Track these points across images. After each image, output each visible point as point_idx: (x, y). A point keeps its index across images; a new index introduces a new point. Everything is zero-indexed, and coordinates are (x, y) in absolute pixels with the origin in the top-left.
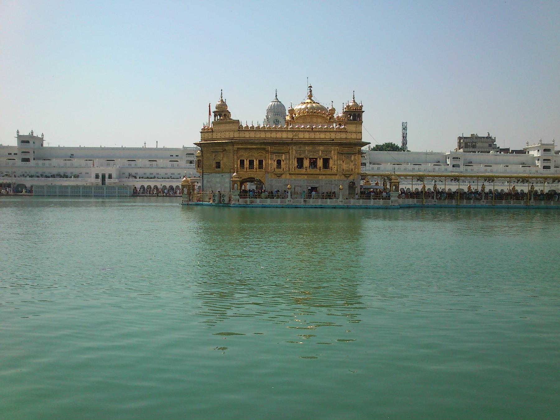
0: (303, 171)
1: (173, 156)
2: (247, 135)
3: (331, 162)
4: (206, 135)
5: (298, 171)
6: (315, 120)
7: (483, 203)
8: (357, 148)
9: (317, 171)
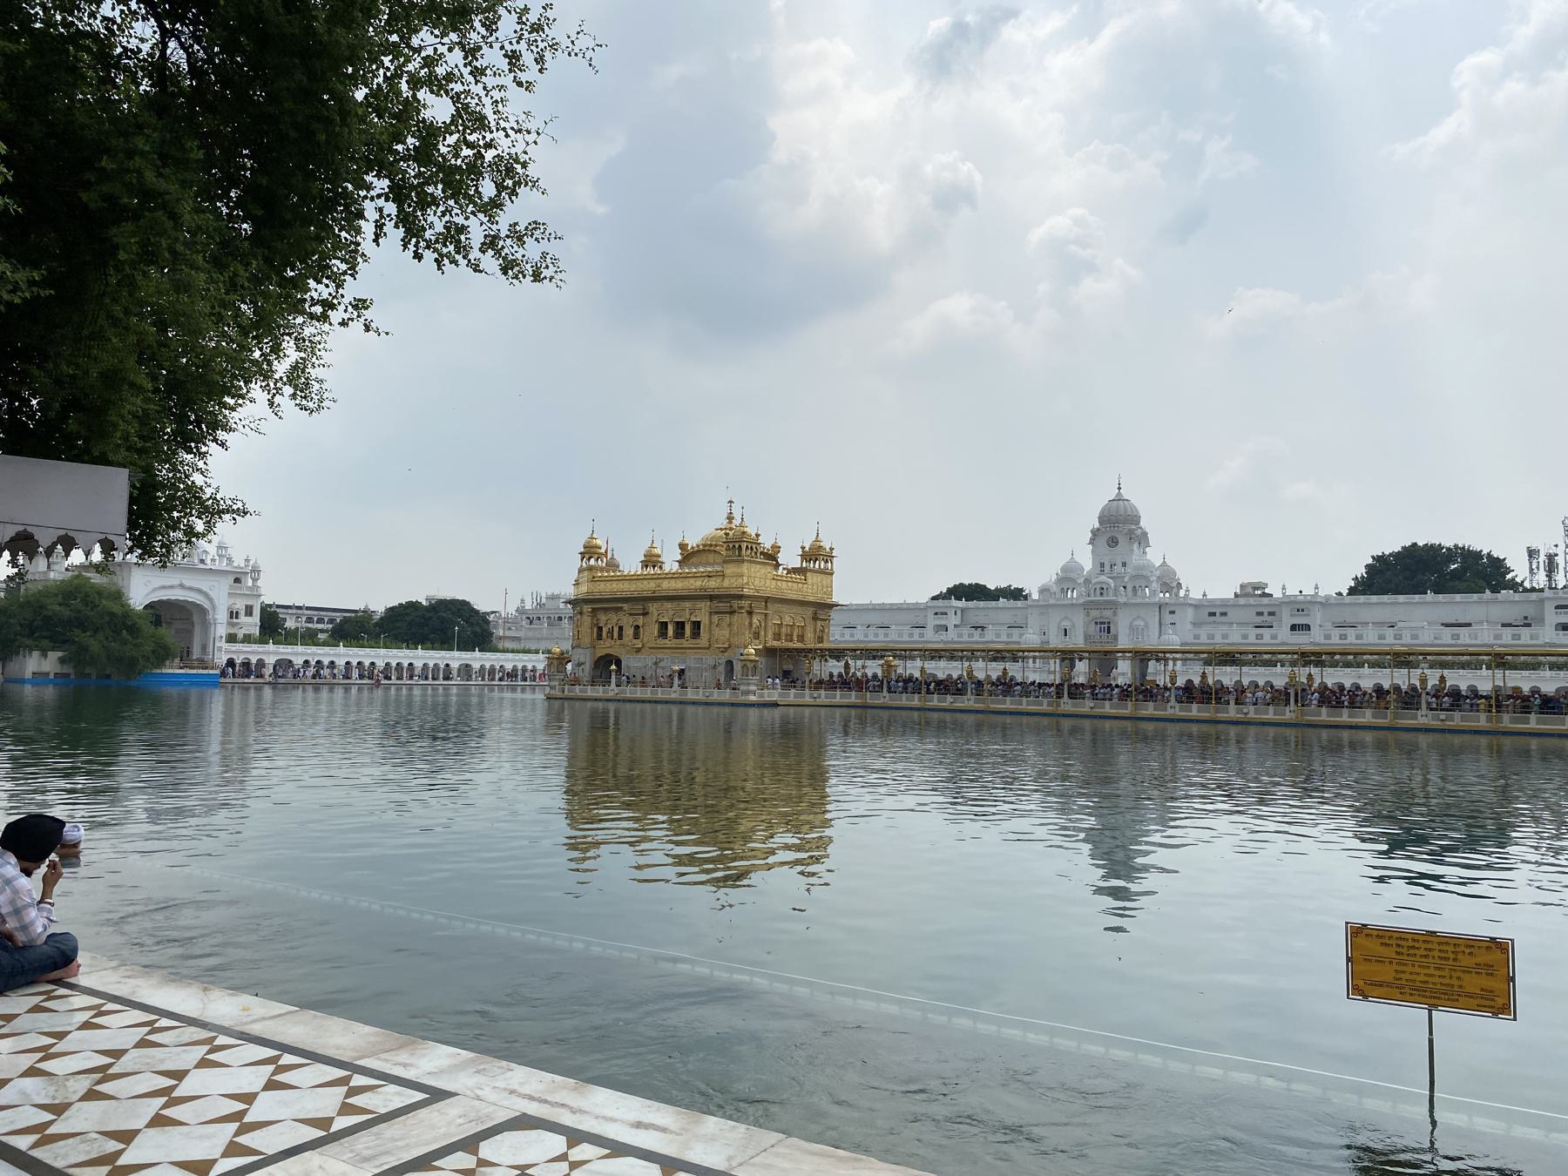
2: (601, 587)
5: (661, 642)
6: (711, 557)
7: (968, 701)
8: (735, 604)
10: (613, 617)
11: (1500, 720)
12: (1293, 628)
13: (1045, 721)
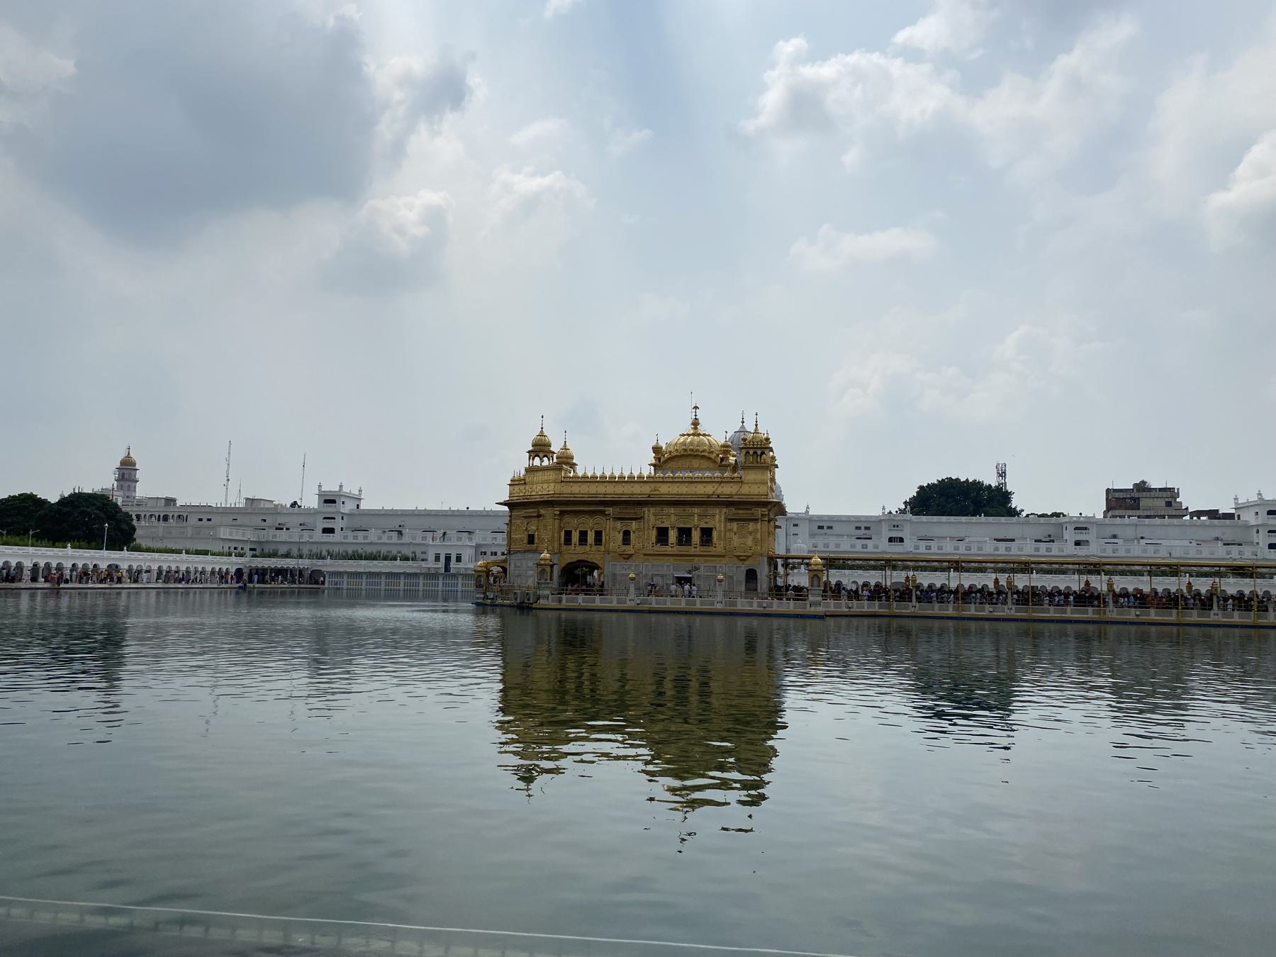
0: (668, 549)
1: (466, 521)
2: (576, 489)
3: (715, 534)
4: (517, 488)
6: (696, 463)
7: (1009, 610)
8: (759, 511)
9: (692, 550)
10: (590, 524)
11: (889, 607)
12: (891, 540)
13: (1091, 627)
